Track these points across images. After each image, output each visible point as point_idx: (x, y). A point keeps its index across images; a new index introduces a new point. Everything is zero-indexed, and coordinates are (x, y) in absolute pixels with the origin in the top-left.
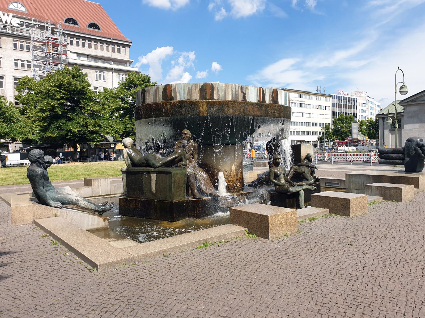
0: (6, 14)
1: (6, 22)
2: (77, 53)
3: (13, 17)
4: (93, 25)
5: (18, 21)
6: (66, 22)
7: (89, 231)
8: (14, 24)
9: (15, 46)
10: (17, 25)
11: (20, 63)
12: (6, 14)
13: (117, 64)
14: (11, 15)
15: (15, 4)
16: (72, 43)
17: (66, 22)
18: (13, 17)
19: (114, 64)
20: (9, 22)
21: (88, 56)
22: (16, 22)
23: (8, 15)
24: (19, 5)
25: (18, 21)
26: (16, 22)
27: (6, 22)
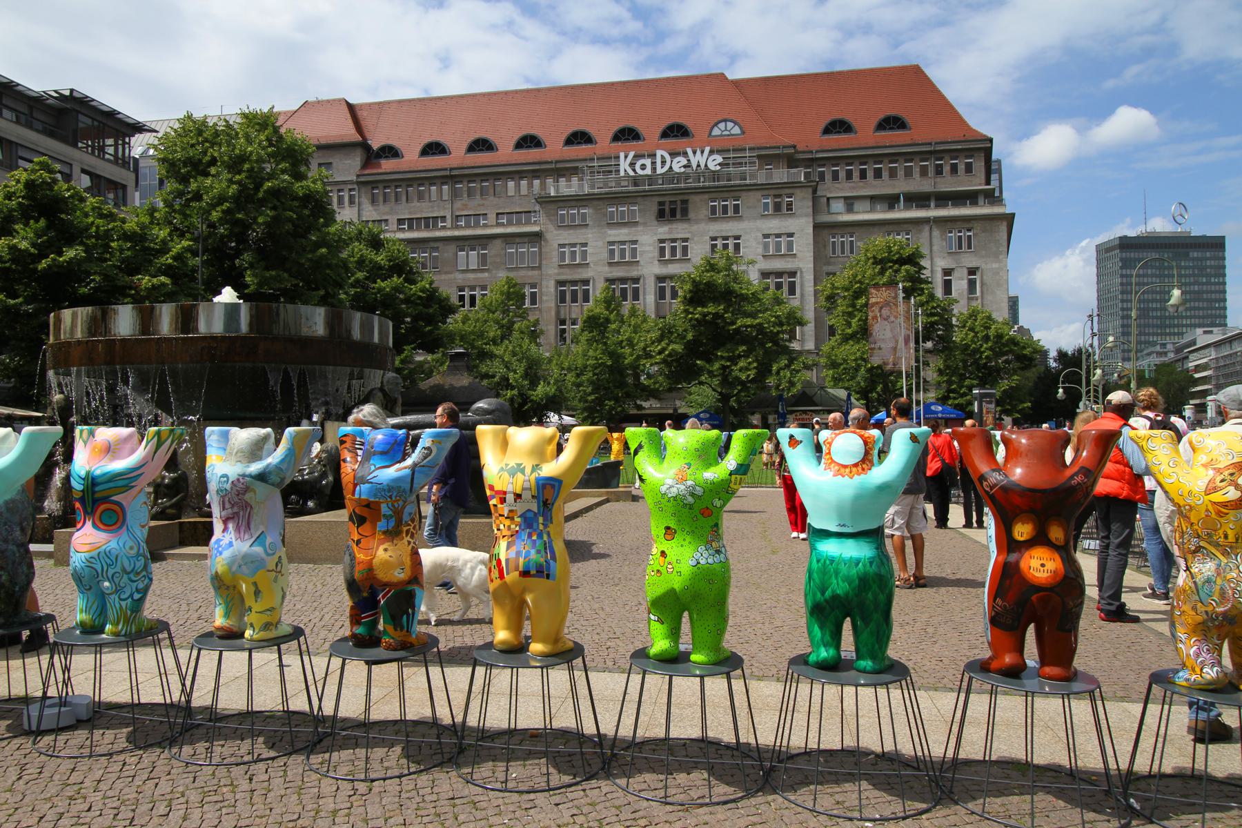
0: (698, 152)
1: (699, 166)
2: (846, 198)
3: (711, 152)
4: (892, 123)
5: (719, 159)
6: (827, 131)
7: (609, 556)
8: (713, 166)
9: (713, 209)
10: (718, 168)
11: (719, 243)
12: (698, 152)
13: (964, 205)
14: (707, 149)
15: (722, 126)
16: (835, 176)
17: (827, 131)
18: (711, 152)
19: (954, 205)
20: (703, 166)
21: (873, 199)
22: (715, 162)
23: (702, 152)
24: (730, 125)
25: (719, 159)
26: (715, 162)
27: (699, 166)
